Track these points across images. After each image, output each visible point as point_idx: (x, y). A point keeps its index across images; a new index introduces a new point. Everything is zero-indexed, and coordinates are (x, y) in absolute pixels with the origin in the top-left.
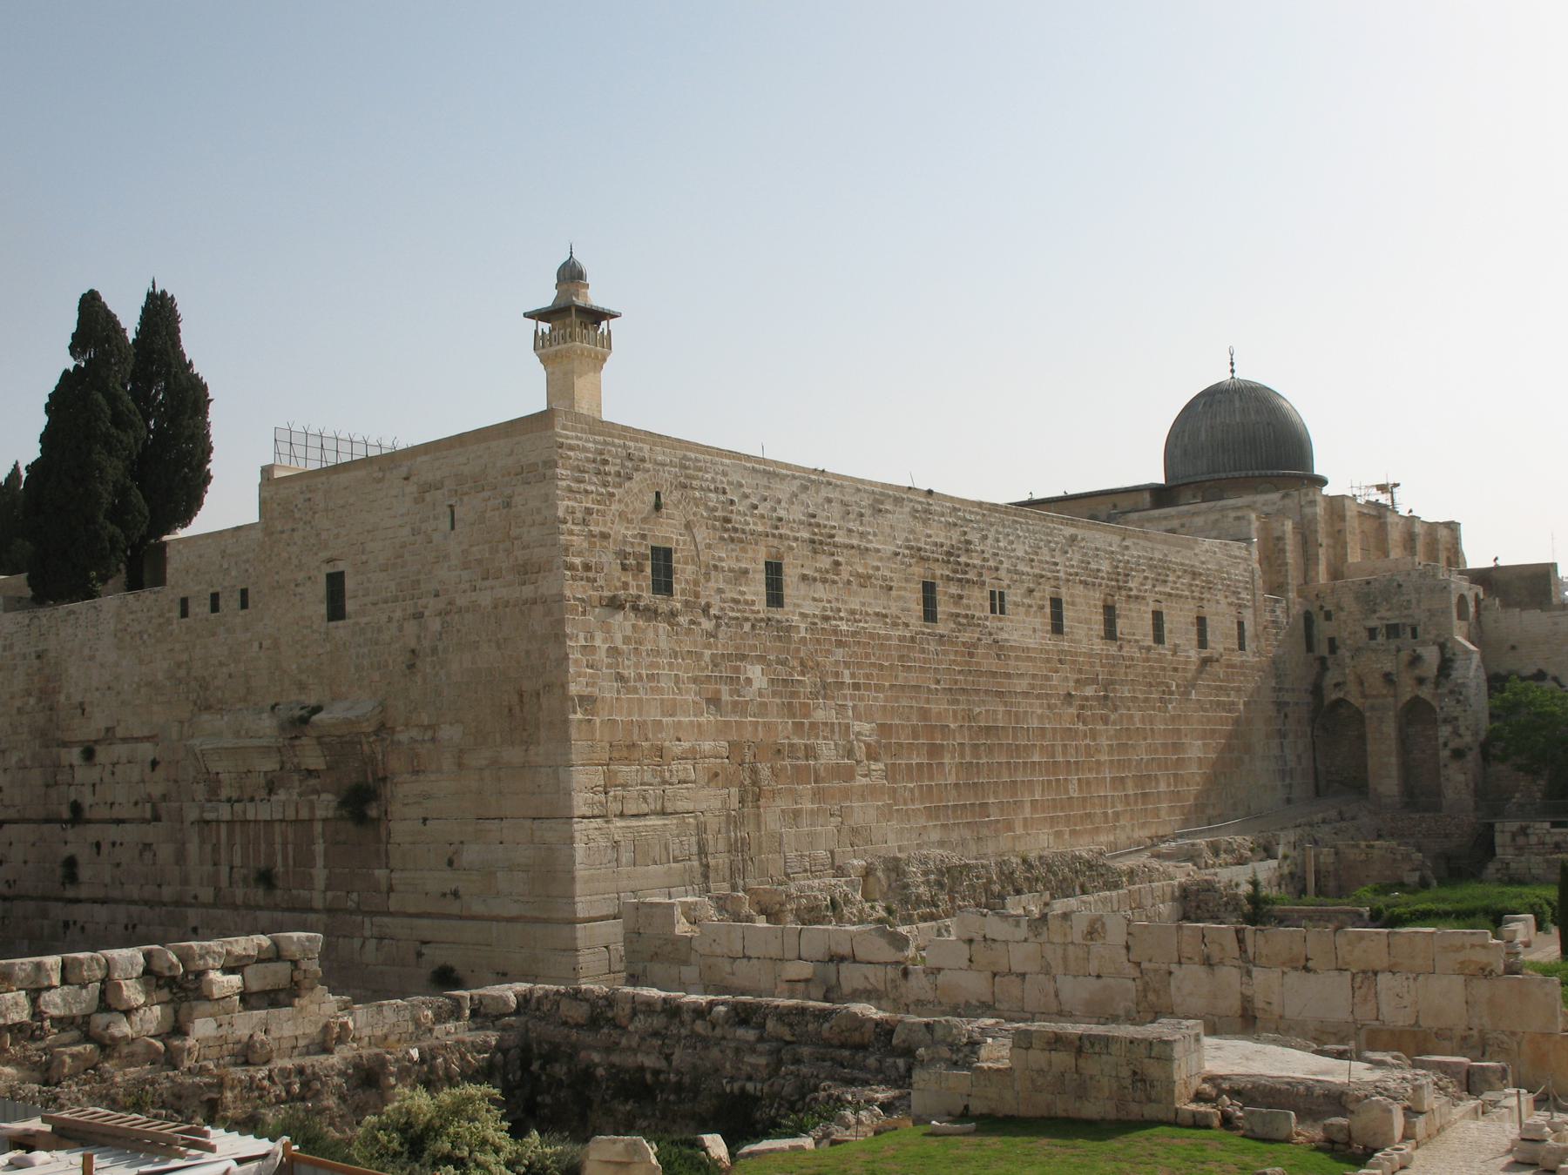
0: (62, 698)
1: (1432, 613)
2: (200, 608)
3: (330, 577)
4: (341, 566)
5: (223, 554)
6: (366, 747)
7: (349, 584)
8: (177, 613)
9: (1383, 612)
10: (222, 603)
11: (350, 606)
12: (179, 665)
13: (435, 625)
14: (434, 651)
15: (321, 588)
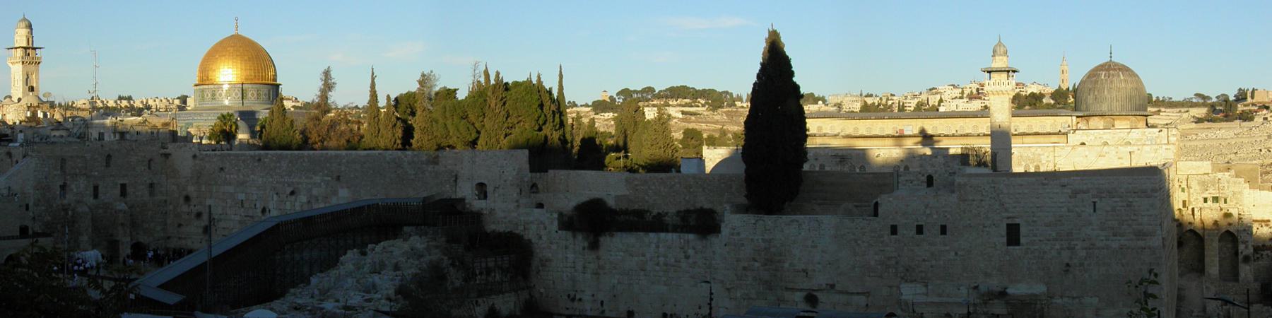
0: (786, 265)
1: (1234, 193)
2: (907, 233)
3: (1008, 225)
4: (1017, 221)
5: (927, 206)
6: (1038, 306)
7: (1023, 230)
8: (889, 231)
9: (1211, 190)
10: (925, 230)
11: (1022, 240)
12: (889, 258)
13: (1083, 253)
14: (1081, 265)
15: (1004, 233)
